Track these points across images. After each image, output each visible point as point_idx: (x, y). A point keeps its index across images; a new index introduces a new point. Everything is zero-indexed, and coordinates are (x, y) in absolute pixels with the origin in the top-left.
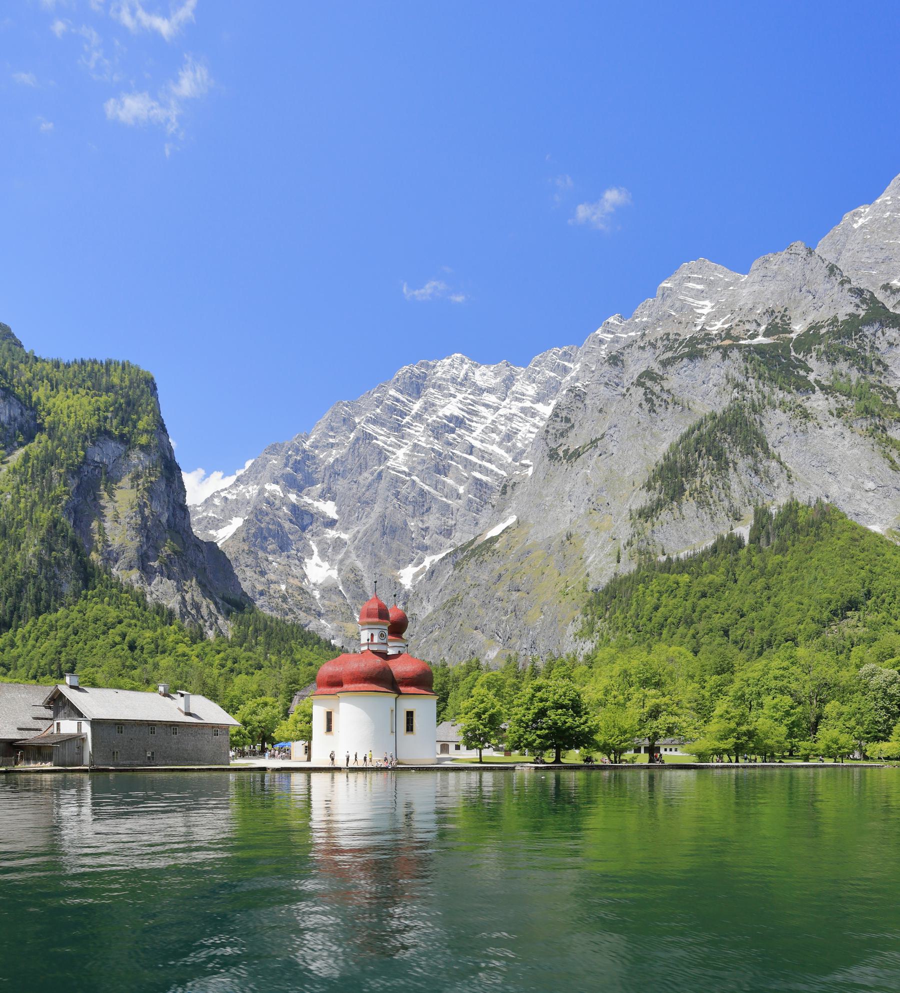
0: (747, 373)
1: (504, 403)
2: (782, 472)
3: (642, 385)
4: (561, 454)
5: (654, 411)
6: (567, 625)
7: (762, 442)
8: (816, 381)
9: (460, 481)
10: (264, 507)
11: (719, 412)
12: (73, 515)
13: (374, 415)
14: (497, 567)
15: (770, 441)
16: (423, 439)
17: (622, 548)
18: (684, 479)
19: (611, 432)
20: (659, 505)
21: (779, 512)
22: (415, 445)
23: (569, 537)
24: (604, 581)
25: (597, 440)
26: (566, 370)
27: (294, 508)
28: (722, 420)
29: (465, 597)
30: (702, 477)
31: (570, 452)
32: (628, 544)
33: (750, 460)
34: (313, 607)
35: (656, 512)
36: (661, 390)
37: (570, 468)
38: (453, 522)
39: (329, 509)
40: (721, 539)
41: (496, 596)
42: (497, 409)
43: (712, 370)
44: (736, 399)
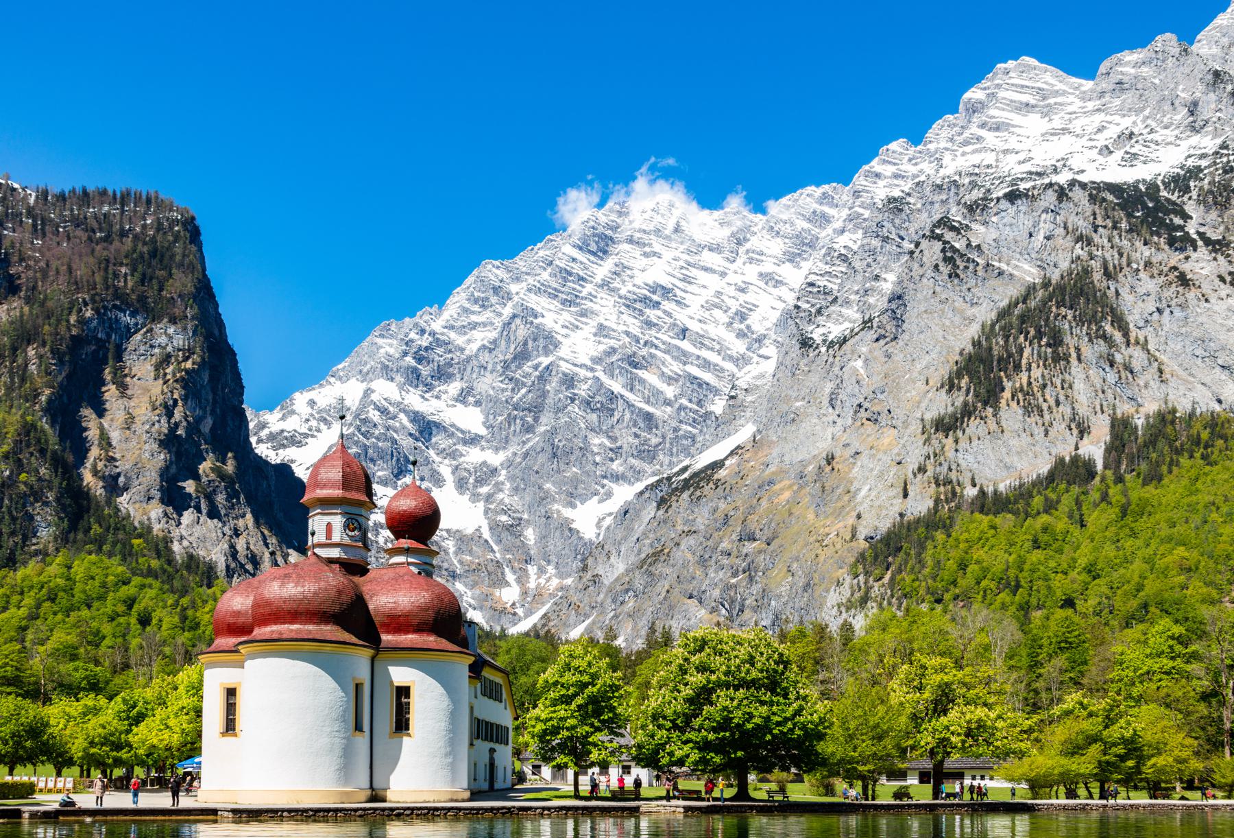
0: (1095, 219)
1: (733, 267)
3: (939, 238)
6: (828, 591)
7: (1120, 322)
8: (1198, 233)
9: (670, 380)
10: (374, 415)
11: (1055, 277)
12: (59, 420)
13: (539, 282)
14: (722, 505)
15: (1133, 319)
16: (614, 318)
17: (911, 476)
18: (1002, 374)
20: (967, 412)
21: (1148, 423)
22: (601, 327)
23: (830, 459)
24: (884, 525)
26: (825, 219)
27: (416, 417)
28: (1061, 288)
29: (674, 549)
30: (1029, 370)
32: (920, 469)
33: (1101, 346)
34: (445, 565)
35: (962, 424)
37: (831, 359)
39: (470, 419)
40: (1060, 462)
41: (720, 548)
42: (723, 274)
43: (1044, 216)
44: (1078, 258)
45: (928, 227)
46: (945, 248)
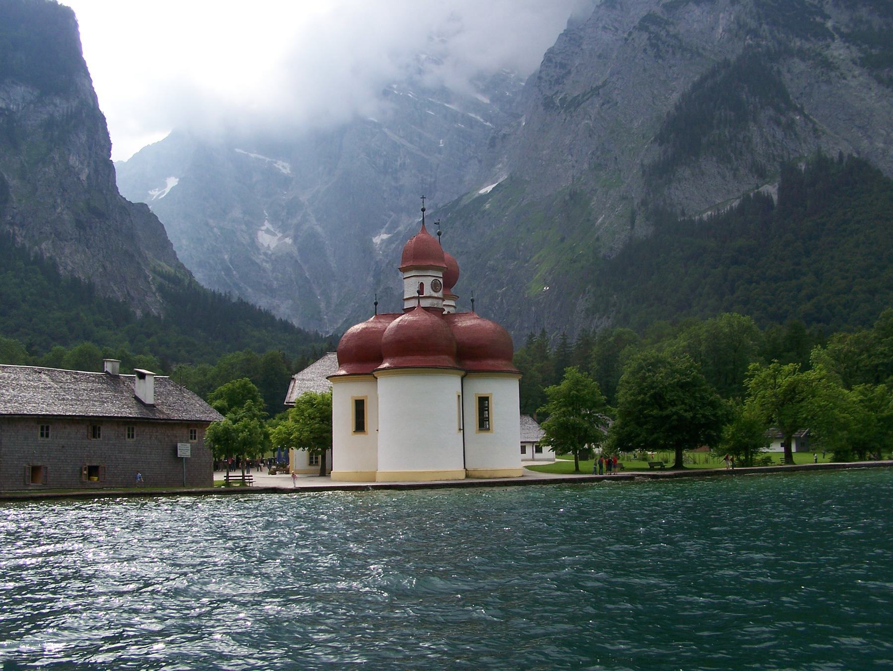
2: (806, 124)
3: (646, 29)
4: (557, 102)
5: (661, 57)
11: (733, 58)
19: (614, 79)
25: (598, 88)
31: (569, 99)
36: (666, 36)
37: (568, 118)
38: (433, 180)
40: (746, 199)
44: (749, 46)
45: (636, 23)
46: (650, 37)
